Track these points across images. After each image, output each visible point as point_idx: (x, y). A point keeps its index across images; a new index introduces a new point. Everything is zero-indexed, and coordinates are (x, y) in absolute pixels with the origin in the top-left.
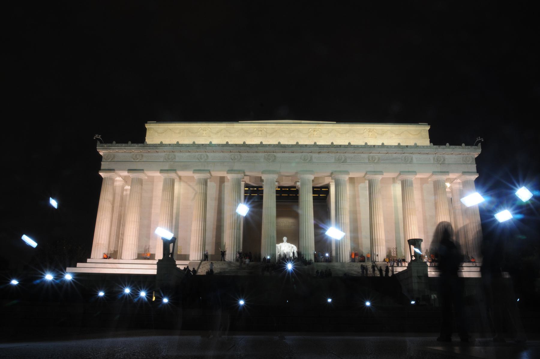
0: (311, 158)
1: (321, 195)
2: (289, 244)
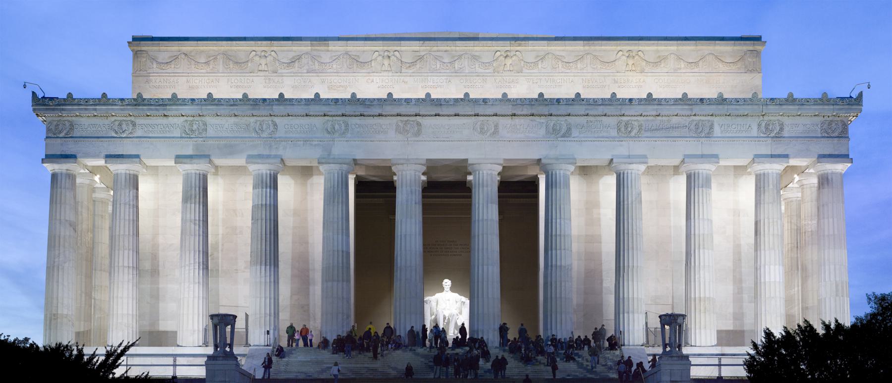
0: (496, 126)
2: (456, 295)
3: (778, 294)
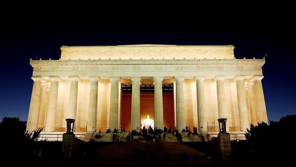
1: (168, 90)
3: (246, 115)
